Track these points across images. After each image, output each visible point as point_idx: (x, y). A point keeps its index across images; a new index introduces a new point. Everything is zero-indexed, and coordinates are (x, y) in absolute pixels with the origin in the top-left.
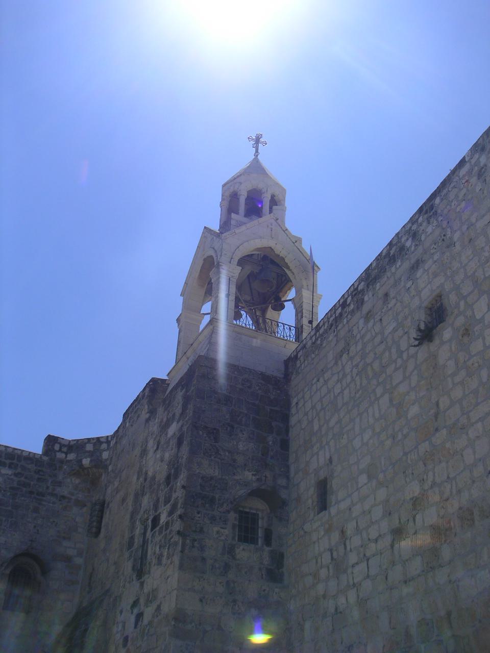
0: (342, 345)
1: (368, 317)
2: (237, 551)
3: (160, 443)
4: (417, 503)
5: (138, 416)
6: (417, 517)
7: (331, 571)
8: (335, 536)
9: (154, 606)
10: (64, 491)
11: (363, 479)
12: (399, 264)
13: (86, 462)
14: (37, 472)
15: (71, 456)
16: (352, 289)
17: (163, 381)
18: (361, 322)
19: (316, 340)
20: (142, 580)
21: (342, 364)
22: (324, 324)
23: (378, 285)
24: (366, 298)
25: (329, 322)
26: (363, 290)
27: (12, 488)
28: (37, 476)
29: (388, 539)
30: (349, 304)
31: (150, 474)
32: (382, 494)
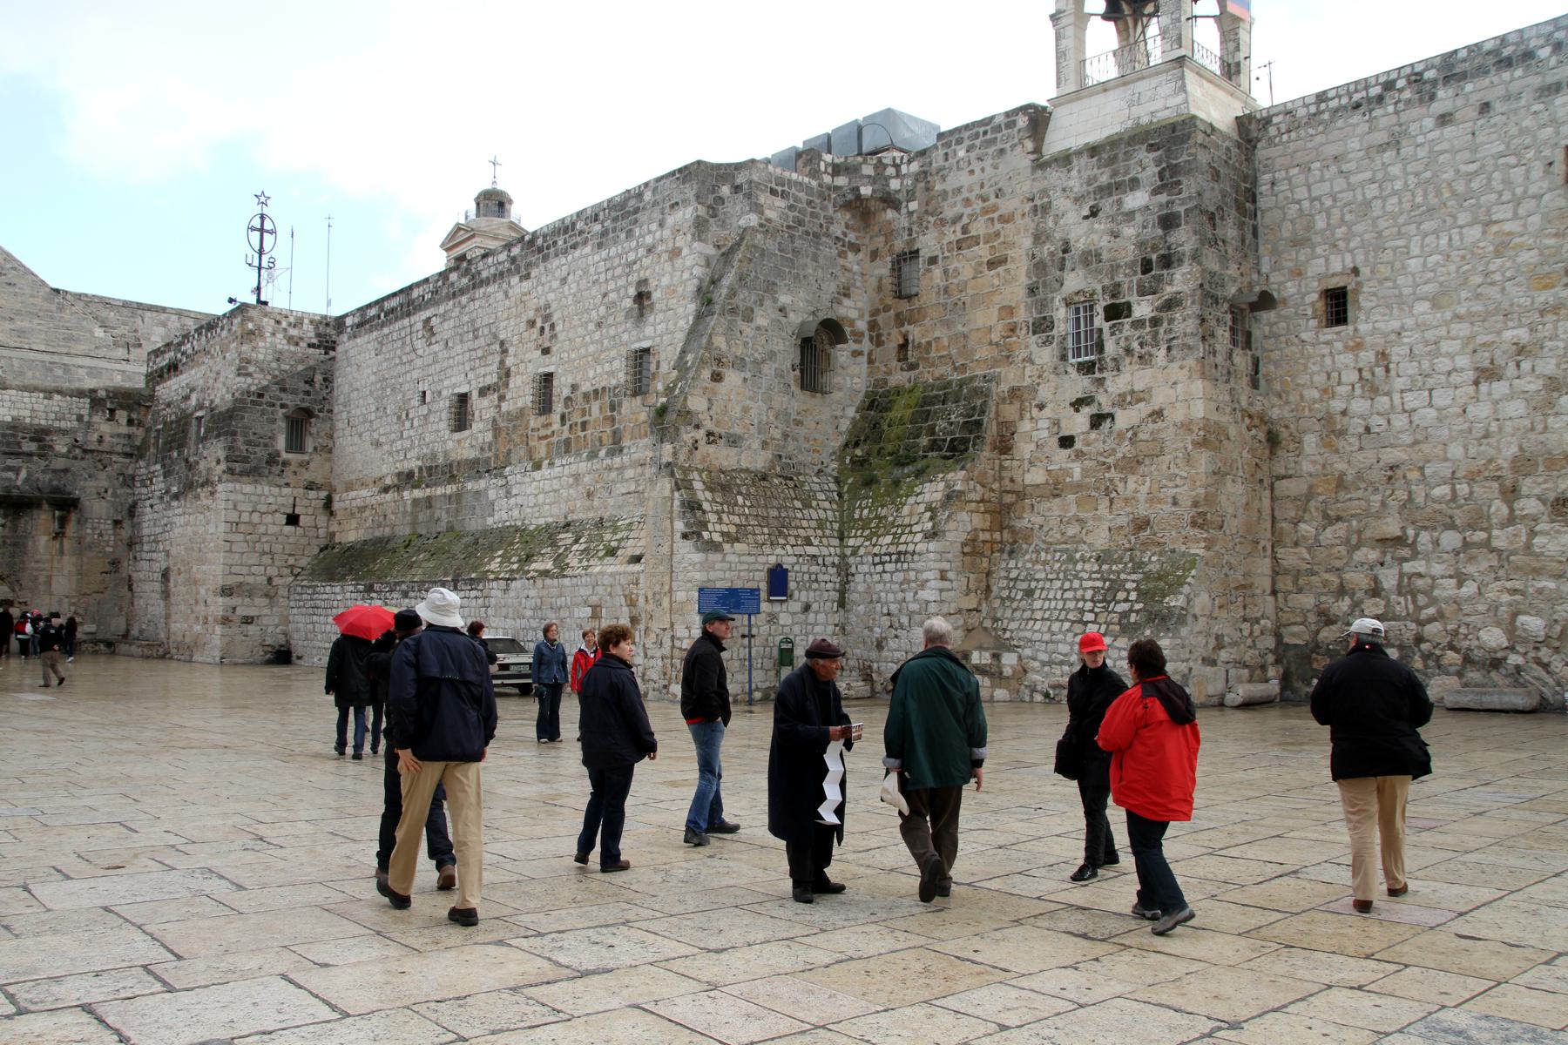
0: (1381, 137)
1: (1444, 119)
2: (1234, 355)
3: (1098, 211)
4: (1521, 350)
5: (1002, 151)
6: (1523, 365)
7: (1358, 391)
8: (1368, 356)
9: (1143, 409)
10: (837, 230)
11: (1422, 307)
13: (866, 191)
14: (810, 203)
15: (841, 181)
16: (1409, 70)
17: (1044, 109)
18: (1429, 123)
19: (1318, 113)
20: (1097, 375)
21: (1383, 164)
22: (1339, 97)
23: (1469, 87)
24: (1441, 93)
25: (1351, 98)
26: (1434, 82)
27: (789, 227)
28: (810, 210)
29: (1471, 375)
30: (1401, 90)
31: (1079, 246)
32: (1462, 329)
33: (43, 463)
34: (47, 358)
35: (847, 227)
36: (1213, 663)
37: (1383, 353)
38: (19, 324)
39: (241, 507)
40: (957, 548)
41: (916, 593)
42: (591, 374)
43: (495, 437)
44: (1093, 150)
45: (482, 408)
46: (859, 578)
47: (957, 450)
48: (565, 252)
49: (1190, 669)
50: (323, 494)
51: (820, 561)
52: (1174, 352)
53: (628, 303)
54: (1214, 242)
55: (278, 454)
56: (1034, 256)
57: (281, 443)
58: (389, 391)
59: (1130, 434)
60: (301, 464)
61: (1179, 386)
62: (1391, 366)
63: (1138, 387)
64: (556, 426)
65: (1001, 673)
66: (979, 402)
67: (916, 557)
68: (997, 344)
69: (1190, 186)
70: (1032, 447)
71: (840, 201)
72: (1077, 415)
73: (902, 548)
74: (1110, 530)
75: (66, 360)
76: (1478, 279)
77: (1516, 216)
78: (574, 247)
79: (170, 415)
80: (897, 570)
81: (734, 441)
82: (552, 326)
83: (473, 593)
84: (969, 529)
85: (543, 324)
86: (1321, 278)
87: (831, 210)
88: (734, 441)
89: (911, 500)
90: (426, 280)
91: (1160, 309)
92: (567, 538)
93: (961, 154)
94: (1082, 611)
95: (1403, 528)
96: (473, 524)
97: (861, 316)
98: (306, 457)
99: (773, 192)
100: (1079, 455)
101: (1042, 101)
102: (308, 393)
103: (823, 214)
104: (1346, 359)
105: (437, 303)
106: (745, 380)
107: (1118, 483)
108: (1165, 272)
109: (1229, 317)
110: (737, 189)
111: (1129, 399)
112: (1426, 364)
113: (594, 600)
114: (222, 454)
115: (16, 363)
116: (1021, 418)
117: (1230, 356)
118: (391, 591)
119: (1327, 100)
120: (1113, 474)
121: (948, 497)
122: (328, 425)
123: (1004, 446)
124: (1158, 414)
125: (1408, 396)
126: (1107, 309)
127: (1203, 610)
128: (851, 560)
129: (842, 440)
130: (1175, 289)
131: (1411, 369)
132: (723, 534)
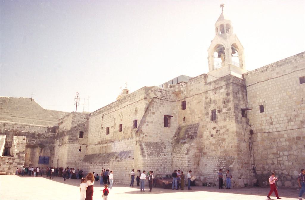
5: (199, 82)
6: (296, 119)
8: (268, 118)
10: (171, 97)
11: (277, 108)
12: (289, 65)
13: (177, 90)
14: (166, 93)
15: (172, 89)
16: (271, 65)
17: (207, 74)
20: (217, 123)
24: (277, 69)
28: (166, 94)
29: (287, 121)
30: (270, 68)
31: (213, 99)
33: (38, 140)
34: (42, 121)
35: (174, 97)
36: (240, 178)
37: (271, 117)
38: (38, 115)
39: (71, 148)
40: (192, 156)
41: (184, 165)
42: (128, 124)
43: (113, 135)
44: (215, 82)
45: (111, 130)
46: (175, 162)
47: (192, 138)
48: (124, 103)
49: (235, 180)
50: (86, 145)
51: (167, 159)
52: (230, 118)
53: (134, 112)
54: (237, 98)
55: (78, 138)
56: (205, 101)
57: (79, 136)
58: (97, 127)
59: (223, 134)
60: (82, 140)
61: (231, 125)
62: (273, 120)
63: (224, 125)
64: (123, 134)
65: (200, 180)
66: (197, 128)
67: (184, 158)
68: (200, 118)
69: (231, 88)
70: (206, 137)
71: (172, 92)
72: (214, 131)
73: (182, 156)
74: (220, 152)
75: (45, 121)
76: (286, 103)
77: (292, 91)
78: (126, 102)
79: (61, 131)
80: (181, 161)
81: (151, 137)
82: (122, 116)
83: (107, 165)
84: (194, 152)
85: (121, 115)
86: (259, 103)
87: (170, 94)
88: (151, 137)
89: (184, 147)
90: (103, 107)
91: (227, 110)
92: (123, 154)
93: (193, 83)
94: (215, 168)
95: (277, 151)
96: (109, 151)
97: (177, 113)
98: (83, 139)
99: (159, 91)
100: (215, 138)
101: (206, 73)
102: (84, 127)
103: (168, 95)
104: (264, 119)
105: (105, 111)
106: (153, 125)
107: (221, 143)
108: (228, 104)
109: (241, 112)
110: (152, 91)
111: (222, 127)
112: (278, 119)
113: (126, 166)
114: (68, 138)
115: (37, 121)
116: (204, 131)
117: (241, 119)
118: (95, 164)
119: (257, 70)
120: (220, 141)
121: (190, 146)
122: (87, 133)
123: (201, 136)
124: (228, 130)
125: (276, 125)
126: (218, 111)
127: (237, 168)
128: (173, 159)
129: (174, 135)
130: (230, 107)
131: (276, 120)
132: (147, 154)
